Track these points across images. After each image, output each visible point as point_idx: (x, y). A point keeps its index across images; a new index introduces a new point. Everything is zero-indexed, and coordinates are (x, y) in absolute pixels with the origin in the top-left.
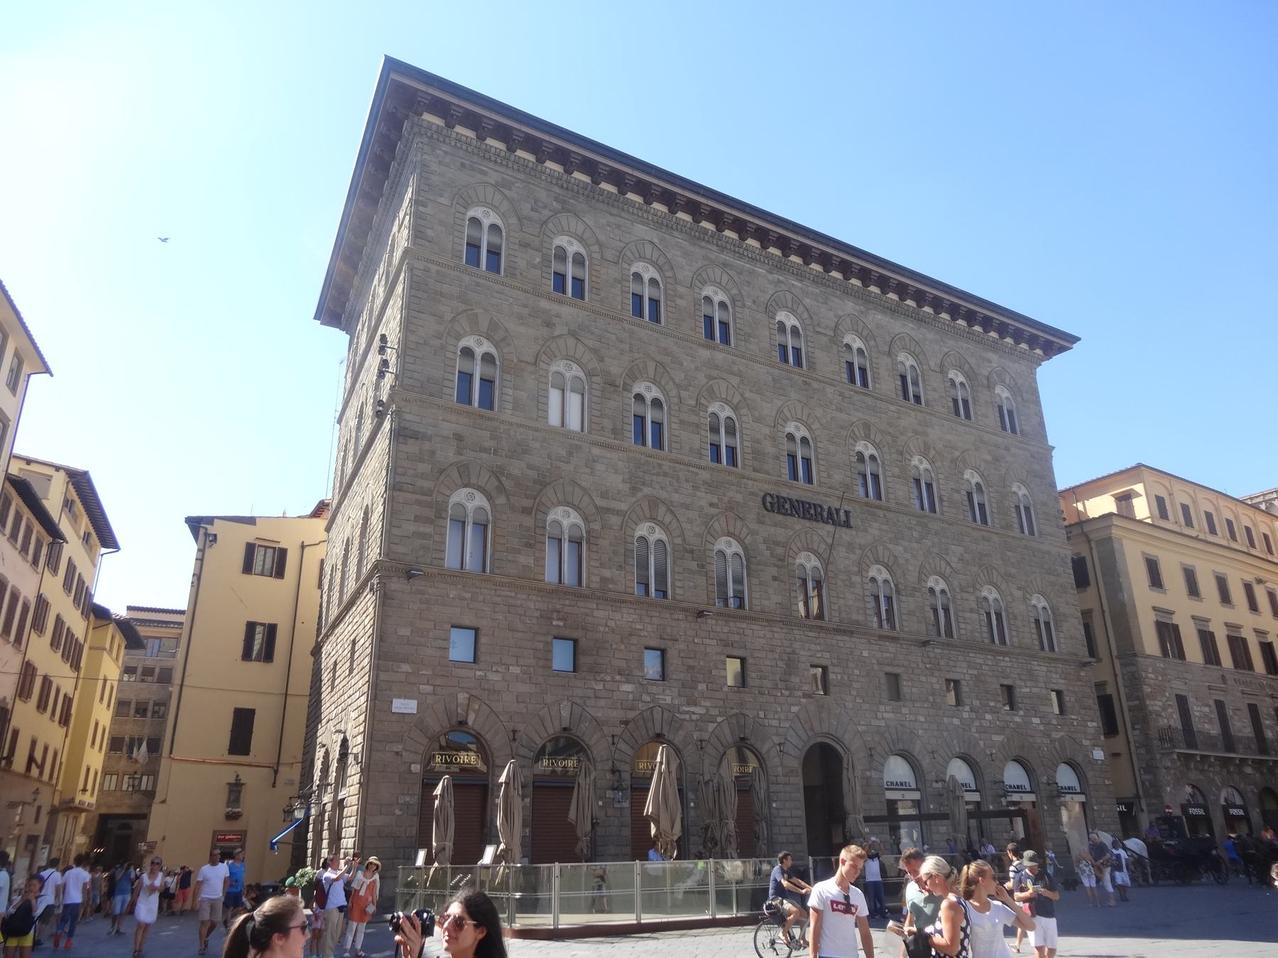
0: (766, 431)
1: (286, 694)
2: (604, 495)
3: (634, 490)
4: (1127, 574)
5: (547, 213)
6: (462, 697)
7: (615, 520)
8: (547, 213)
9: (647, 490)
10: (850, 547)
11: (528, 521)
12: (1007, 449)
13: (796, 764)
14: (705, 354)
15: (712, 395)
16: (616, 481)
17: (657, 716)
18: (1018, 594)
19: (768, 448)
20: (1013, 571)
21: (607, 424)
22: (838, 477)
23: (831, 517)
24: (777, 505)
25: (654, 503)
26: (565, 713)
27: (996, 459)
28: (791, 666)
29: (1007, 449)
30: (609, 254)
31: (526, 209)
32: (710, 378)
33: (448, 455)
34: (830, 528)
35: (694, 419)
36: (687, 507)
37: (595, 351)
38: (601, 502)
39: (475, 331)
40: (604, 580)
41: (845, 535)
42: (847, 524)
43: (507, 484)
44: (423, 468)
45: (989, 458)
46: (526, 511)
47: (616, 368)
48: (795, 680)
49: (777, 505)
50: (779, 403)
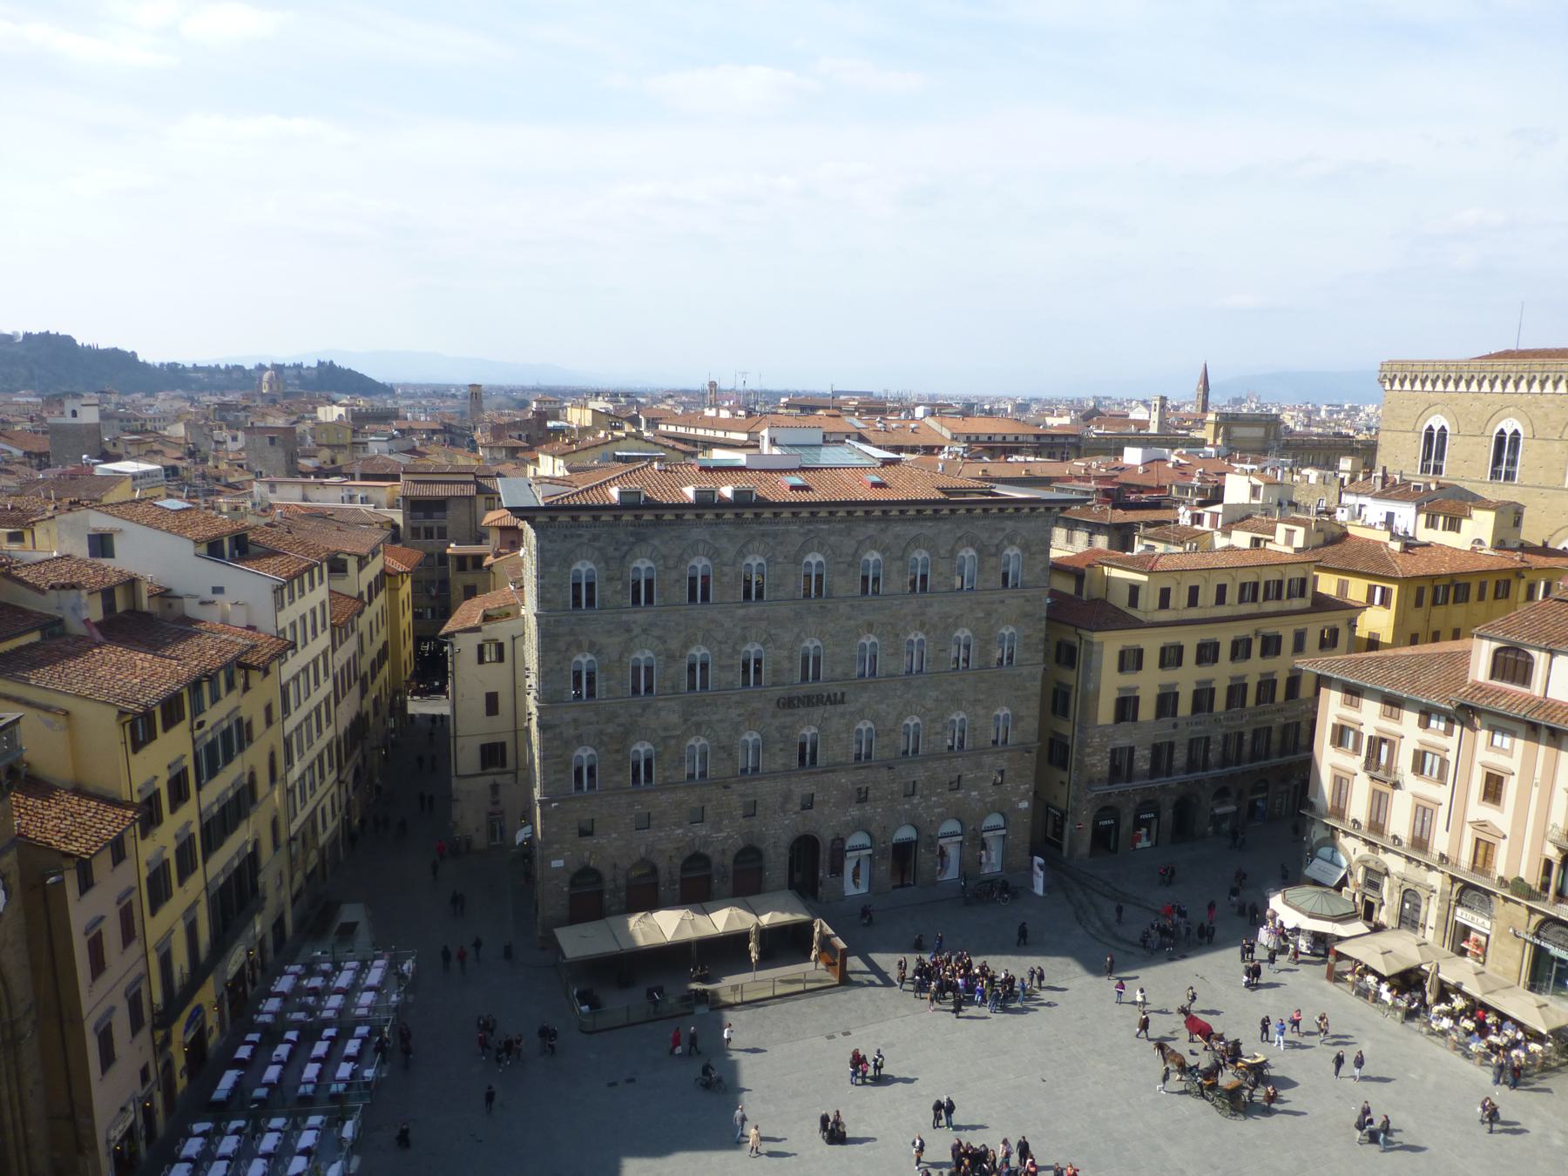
0: (786, 653)
1: (516, 731)
2: (665, 729)
3: (686, 721)
4: (1099, 670)
5: (625, 548)
6: (587, 854)
7: (673, 742)
8: (625, 548)
9: (694, 719)
10: (842, 715)
11: (619, 757)
12: (1002, 602)
13: (784, 851)
14: (741, 612)
15: (745, 640)
16: (674, 719)
17: (697, 842)
18: (981, 712)
19: (786, 665)
20: (982, 697)
21: (668, 684)
22: (839, 670)
23: (834, 700)
24: (788, 703)
25: (698, 725)
26: (642, 850)
27: (989, 614)
28: (787, 798)
29: (1002, 602)
30: (671, 563)
31: (610, 551)
32: (744, 628)
33: (570, 732)
34: (829, 707)
35: (730, 662)
36: (721, 721)
37: (659, 638)
38: (662, 734)
39: (580, 648)
40: (665, 778)
41: (840, 708)
42: (842, 702)
43: (605, 739)
44: (556, 743)
45: (981, 615)
46: (617, 751)
47: (674, 645)
48: (790, 806)
49: (788, 703)
50: (796, 630)
